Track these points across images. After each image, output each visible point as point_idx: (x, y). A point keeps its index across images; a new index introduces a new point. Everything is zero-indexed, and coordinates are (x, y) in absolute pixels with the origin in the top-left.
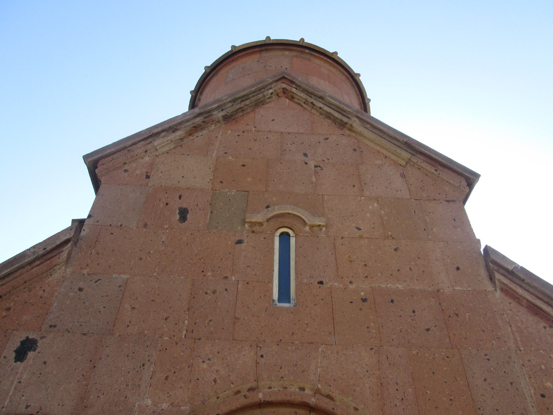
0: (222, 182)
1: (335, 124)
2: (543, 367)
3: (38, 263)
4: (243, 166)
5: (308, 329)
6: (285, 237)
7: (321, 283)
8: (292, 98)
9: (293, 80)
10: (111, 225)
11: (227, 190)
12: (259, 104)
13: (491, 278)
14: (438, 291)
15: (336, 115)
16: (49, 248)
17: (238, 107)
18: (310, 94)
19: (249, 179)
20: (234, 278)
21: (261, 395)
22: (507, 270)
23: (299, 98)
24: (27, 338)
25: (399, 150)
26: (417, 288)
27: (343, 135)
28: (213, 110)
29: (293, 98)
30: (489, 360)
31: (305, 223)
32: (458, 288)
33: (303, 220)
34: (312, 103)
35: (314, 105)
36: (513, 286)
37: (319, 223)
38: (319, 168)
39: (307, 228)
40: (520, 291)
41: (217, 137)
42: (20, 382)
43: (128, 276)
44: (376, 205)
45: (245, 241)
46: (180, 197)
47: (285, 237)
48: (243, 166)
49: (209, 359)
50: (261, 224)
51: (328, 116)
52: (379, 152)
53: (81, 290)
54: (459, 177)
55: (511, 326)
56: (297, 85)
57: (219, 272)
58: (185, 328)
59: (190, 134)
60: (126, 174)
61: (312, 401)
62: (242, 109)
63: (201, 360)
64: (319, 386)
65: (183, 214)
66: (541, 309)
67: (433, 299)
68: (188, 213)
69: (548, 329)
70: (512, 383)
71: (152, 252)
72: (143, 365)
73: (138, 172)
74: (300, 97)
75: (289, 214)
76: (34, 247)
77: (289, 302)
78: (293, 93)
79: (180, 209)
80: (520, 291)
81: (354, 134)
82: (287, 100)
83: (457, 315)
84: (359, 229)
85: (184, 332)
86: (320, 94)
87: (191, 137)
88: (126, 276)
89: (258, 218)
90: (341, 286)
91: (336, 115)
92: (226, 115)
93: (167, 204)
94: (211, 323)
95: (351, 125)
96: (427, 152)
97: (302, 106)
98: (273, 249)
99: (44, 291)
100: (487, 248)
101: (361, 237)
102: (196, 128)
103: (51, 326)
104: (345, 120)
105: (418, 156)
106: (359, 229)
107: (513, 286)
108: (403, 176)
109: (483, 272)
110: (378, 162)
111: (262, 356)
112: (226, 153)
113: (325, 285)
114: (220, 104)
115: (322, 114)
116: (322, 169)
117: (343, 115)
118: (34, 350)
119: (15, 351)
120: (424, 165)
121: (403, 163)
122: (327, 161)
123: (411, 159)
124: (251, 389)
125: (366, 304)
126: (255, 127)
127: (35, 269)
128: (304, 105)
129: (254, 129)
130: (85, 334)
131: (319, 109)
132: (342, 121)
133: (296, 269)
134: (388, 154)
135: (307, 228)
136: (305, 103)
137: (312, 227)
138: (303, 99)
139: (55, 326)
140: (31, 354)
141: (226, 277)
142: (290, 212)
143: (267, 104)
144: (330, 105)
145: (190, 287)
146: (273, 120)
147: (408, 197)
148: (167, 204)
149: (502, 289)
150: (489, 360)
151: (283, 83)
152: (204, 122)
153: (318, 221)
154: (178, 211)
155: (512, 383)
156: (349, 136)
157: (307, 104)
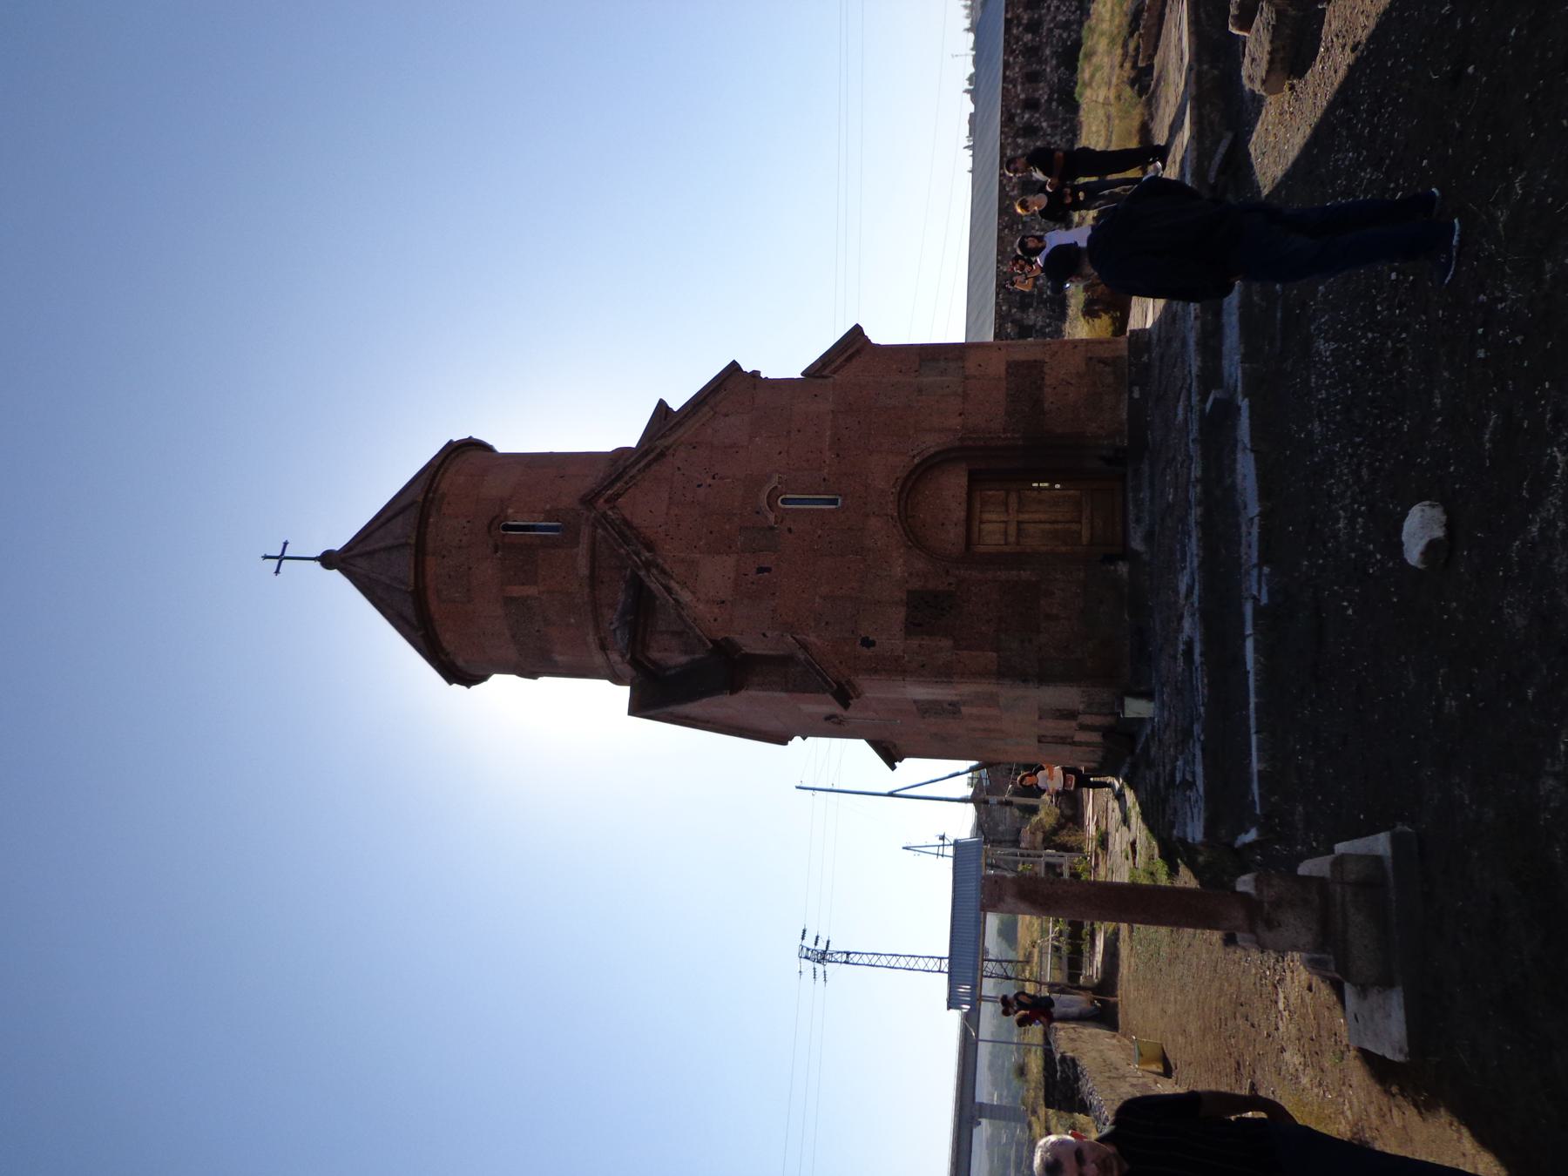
6: (784, 501)
8: (619, 495)
13: (823, 377)
15: (651, 457)
16: (798, 646)
17: (635, 541)
18: (619, 477)
21: (896, 514)
28: (641, 560)
31: (776, 487)
34: (631, 477)
39: (779, 486)
47: (784, 501)
50: (776, 516)
51: (648, 465)
56: (603, 489)
59: (672, 577)
65: (761, 570)
73: (716, 610)
81: (674, 446)
84: (780, 453)
87: (674, 576)
88: (817, 599)
89: (771, 517)
91: (651, 457)
97: (630, 487)
100: (802, 374)
101: (788, 452)
102: (663, 572)
104: (659, 450)
108: (726, 415)
109: (820, 381)
110: (709, 431)
113: (827, 477)
115: (644, 471)
117: (652, 451)
121: (712, 413)
124: (892, 518)
128: (630, 484)
129: (663, 527)
135: (779, 486)
137: (779, 483)
149: (834, 373)
153: (776, 478)
156: (675, 450)
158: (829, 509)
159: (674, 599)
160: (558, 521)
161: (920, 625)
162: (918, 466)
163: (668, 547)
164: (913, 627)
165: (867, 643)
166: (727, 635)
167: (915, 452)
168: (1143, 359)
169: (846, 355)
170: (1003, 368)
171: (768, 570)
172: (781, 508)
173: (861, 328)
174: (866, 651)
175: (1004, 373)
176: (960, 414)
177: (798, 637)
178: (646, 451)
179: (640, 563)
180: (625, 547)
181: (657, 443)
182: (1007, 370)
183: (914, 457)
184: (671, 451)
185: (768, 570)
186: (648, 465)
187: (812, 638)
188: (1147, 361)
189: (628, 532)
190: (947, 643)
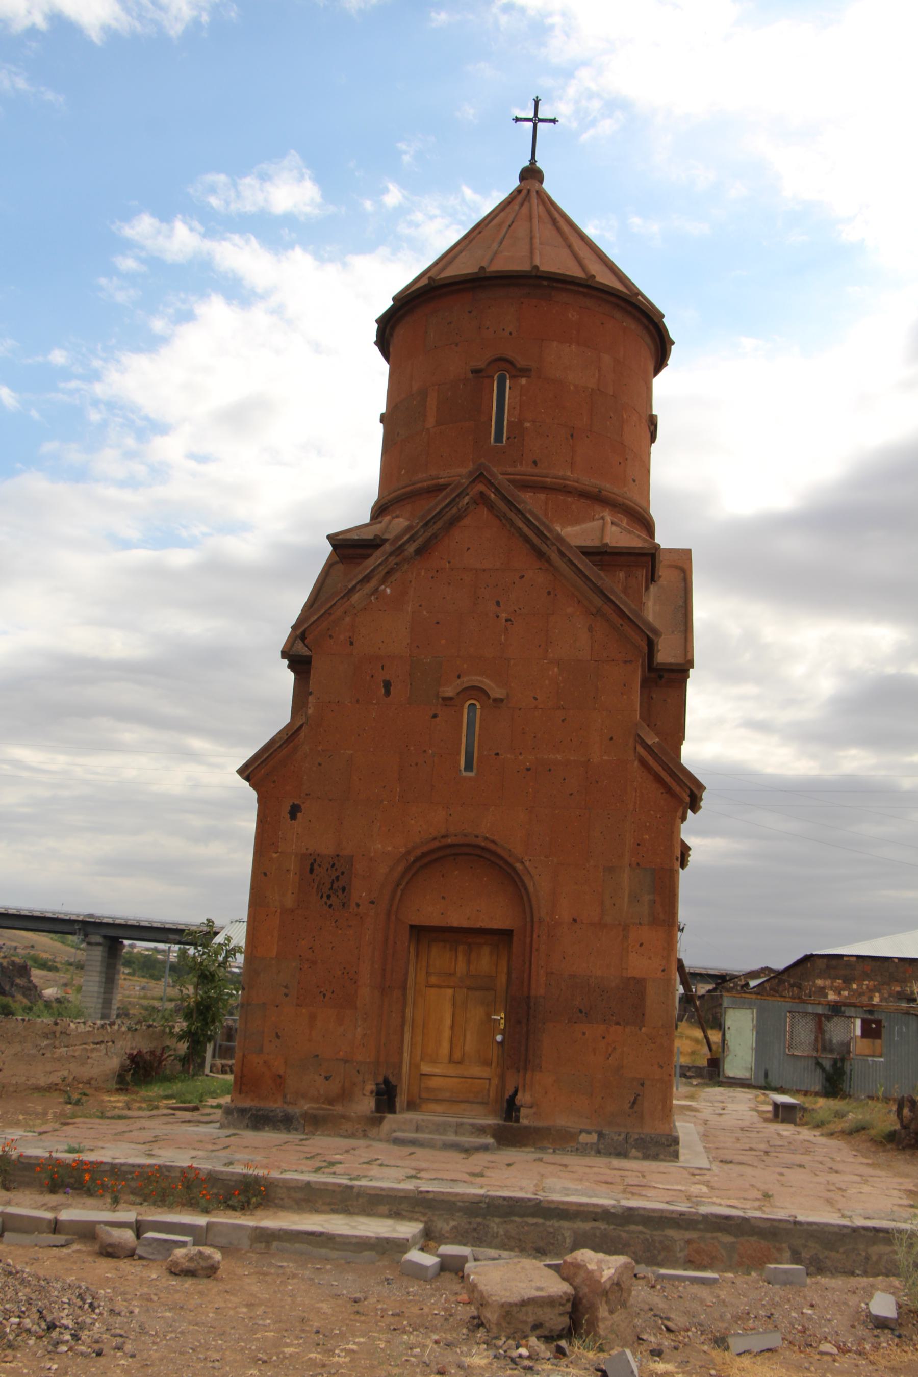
0: (418, 647)
2: (648, 824)
4: (438, 623)
7: (497, 754)
8: (491, 506)
11: (423, 657)
12: (453, 522)
20: (431, 751)
21: (449, 841)
26: (572, 758)
27: (540, 569)
29: (492, 507)
32: (605, 758)
38: (509, 622)
41: (411, 582)
44: (556, 669)
48: (438, 623)
50: (451, 699)
53: (320, 764)
56: (496, 489)
61: (483, 844)
62: (434, 536)
65: (387, 685)
73: (342, 637)
76: (279, 733)
77: (472, 771)
82: (486, 509)
83: (597, 782)
86: (520, 507)
89: (449, 691)
93: (372, 676)
95: (549, 557)
98: (462, 722)
101: (536, 708)
102: (389, 573)
106: (536, 699)
108: (590, 629)
110: (570, 610)
112: (420, 606)
118: (301, 812)
122: (518, 611)
126: (449, 562)
130: (331, 800)
133: (479, 743)
140: (299, 815)
141: (425, 751)
144: (528, 522)
146: (468, 549)
148: (372, 676)
158: (459, 761)
159: (354, 587)
160: (508, 438)
161: (312, 871)
162: (514, 869)
163: (423, 574)
164: (311, 864)
165: (294, 811)
167: (527, 864)
168: (634, 1150)
171: (388, 693)
174: (286, 808)
175: (629, 976)
179: (400, 542)
180: (421, 524)
182: (634, 978)
183: (522, 863)
185: (388, 693)
186: (527, 540)
188: (631, 1155)
189: (440, 524)
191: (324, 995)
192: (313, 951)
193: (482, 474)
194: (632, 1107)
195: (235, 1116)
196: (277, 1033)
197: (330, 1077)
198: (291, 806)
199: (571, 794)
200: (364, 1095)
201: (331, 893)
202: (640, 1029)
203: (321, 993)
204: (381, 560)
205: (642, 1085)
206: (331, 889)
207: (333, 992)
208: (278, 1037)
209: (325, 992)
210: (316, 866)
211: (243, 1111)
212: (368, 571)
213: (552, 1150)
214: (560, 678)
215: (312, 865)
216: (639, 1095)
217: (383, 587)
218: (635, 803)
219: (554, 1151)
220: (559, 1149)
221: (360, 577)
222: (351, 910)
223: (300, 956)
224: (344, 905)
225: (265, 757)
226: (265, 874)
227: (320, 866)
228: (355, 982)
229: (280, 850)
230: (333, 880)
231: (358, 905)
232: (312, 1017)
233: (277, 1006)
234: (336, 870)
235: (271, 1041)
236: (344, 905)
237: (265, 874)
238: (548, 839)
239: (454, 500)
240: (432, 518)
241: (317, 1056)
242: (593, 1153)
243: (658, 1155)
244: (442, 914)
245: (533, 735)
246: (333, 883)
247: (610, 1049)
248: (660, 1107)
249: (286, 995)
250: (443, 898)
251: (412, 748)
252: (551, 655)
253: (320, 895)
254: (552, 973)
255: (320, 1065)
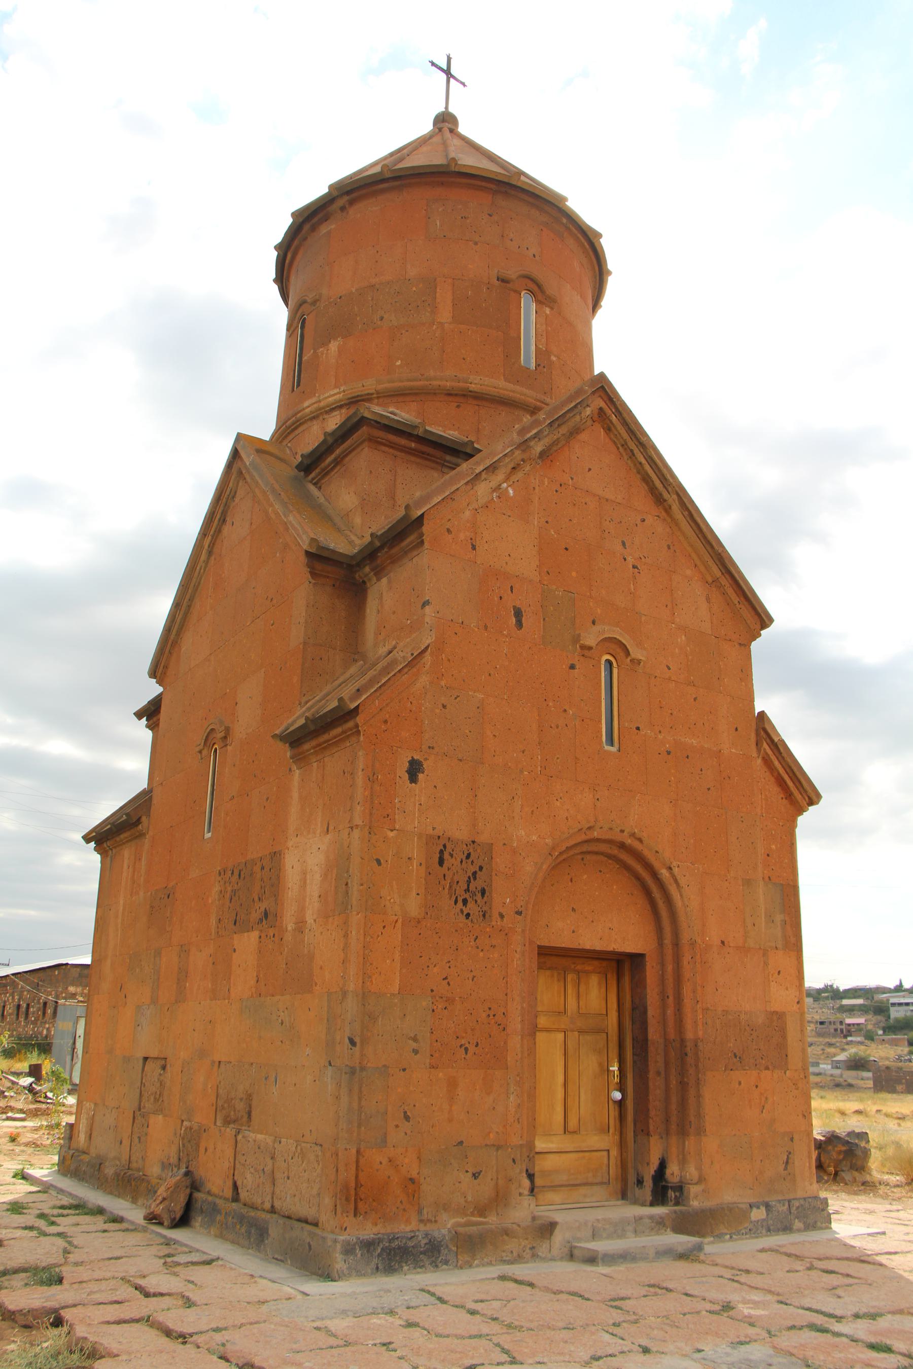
1: (652, 494)
2: (773, 833)
3: (406, 670)
5: (629, 777)
8: (608, 429)
9: (614, 399)
10: (452, 620)
11: (554, 587)
12: (575, 432)
14: (720, 751)
15: (658, 483)
16: (415, 655)
19: (574, 574)
21: (596, 834)
22: (772, 741)
23: (618, 435)
24: (412, 757)
25: (711, 563)
26: (706, 746)
27: (658, 516)
30: (742, 821)
31: (627, 653)
32: (733, 751)
33: (628, 650)
34: (632, 451)
35: (633, 454)
36: (773, 757)
37: (641, 658)
40: (776, 763)
41: (534, 488)
42: (421, 804)
43: (483, 696)
44: (683, 637)
45: (577, 667)
46: (512, 587)
48: (566, 549)
49: (561, 798)
50: (590, 648)
51: (646, 479)
52: (690, 556)
53: (444, 706)
54: (756, 617)
55: (761, 794)
57: (559, 703)
58: (539, 763)
60: (450, 536)
61: (629, 841)
62: (557, 441)
63: (555, 799)
64: (636, 831)
65: (518, 614)
66: (785, 783)
67: (715, 759)
68: (522, 616)
69: (784, 799)
70: (752, 843)
71: (498, 666)
72: (513, 798)
73: (462, 536)
74: (620, 434)
75: (615, 638)
77: (612, 745)
78: (611, 422)
79: (514, 607)
80: (776, 763)
81: (669, 520)
82: (602, 430)
83: (729, 778)
85: (539, 769)
89: (591, 639)
90: (653, 734)
92: (544, 450)
93: (501, 598)
94: (558, 760)
96: (736, 575)
98: (600, 680)
99: (411, 703)
100: (762, 714)
101: (670, 679)
103: (429, 747)
104: (666, 495)
105: (727, 576)
107: (773, 757)
108: (708, 600)
111: (598, 799)
114: (539, 428)
115: (638, 472)
116: (639, 573)
118: (423, 773)
119: (407, 771)
120: (730, 592)
123: (719, 579)
124: (590, 828)
125: (670, 756)
126: (572, 479)
127: (403, 677)
130: (461, 760)
131: (638, 465)
132: (661, 494)
134: (698, 563)
136: (622, 445)
138: (622, 438)
139: (433, 748)
140: (420, 776)
141: (565, 711)
142: (618, 637)
143: (581, 432)
145: (537, 718)
146: (590, 470)
147: (710, 633)
148: (501, 598)
149: (763, 758)
150: (742, 821)
151: (600, 396)
152: (523, 460)
154: (513, 612)
155: (752, 843)
157: (625, 449)
159: (480, 473)
161: (441, 862)
162: (655, 875)
165: (414, 770)
166: (426, 545)
167: (676, 870)
168: (796, 1220)
169: (786, 777)
170: (775, 1007)
171: (519, 624)
172: (601, 656)
173: (817, 803)
176: (723, 942)
177: (427, 657)
178: (666, 479)
179: (528, 436)
181: (675, 497)
182: (777, 1013)
184: (664, 514)
185: (519, 624)
187: (424, 680)
188: (794, 1227)
190: (414, 907)
191: (466, 1050)
192: (449, 984)
193: (602, 387)
194: (785, 1169)
195: (359, 1255)
196: (405, 1113)
197: (479, 1174)
198: (409, 762)
199: (709, 789)
200: (520, 1194)
201: (467, 896)
202: (785, 1073)
203: (461, 1046)
204: (509, 449)
205: (792, 1139)
206: (467, 890)
207: (477, 1045)
208: (407, 1118)
209: (467, 1045)
210: (446, 855)
211: (368, 1245)
212: (496, 458)
213: (728, 1236)
214: (688, 648)
215: (441, 852)
216: (790, 1153)
217: (505, 485)
218: (762, 806)
219: (731, 1237)
220: (734, 1234)
221: (488, 463)
222: (494, 923)
223: (432, 991)
224: (484, 916)
225: (383, 681)
226: (379, 862)
227: (452, 855)
228: (504, 1029)
229: (397, 827)
230: (469, 878)
231: (502, 916)
232: (452, 1084)
233: (404, 1070)
234: (472, 862)
235: (397, 1126)
236: (484, 916)
237: (379, 862)
238: (692, 841)
239: (575, 406)
240: (557, 419)
241: (461, 1143)
242: (764, 1231)
243: (816, 1222)
244: (573, 932)
245: (670, 712)
246: (469, 882)
247: (763, 1099)
248: (808, 1164)
249: (416, 1052)
250: (573, 909)
251: (551, 704)
252: (678, 620)
253: (454, 898)
254: (708, 1009)
255: (466, 1157)
